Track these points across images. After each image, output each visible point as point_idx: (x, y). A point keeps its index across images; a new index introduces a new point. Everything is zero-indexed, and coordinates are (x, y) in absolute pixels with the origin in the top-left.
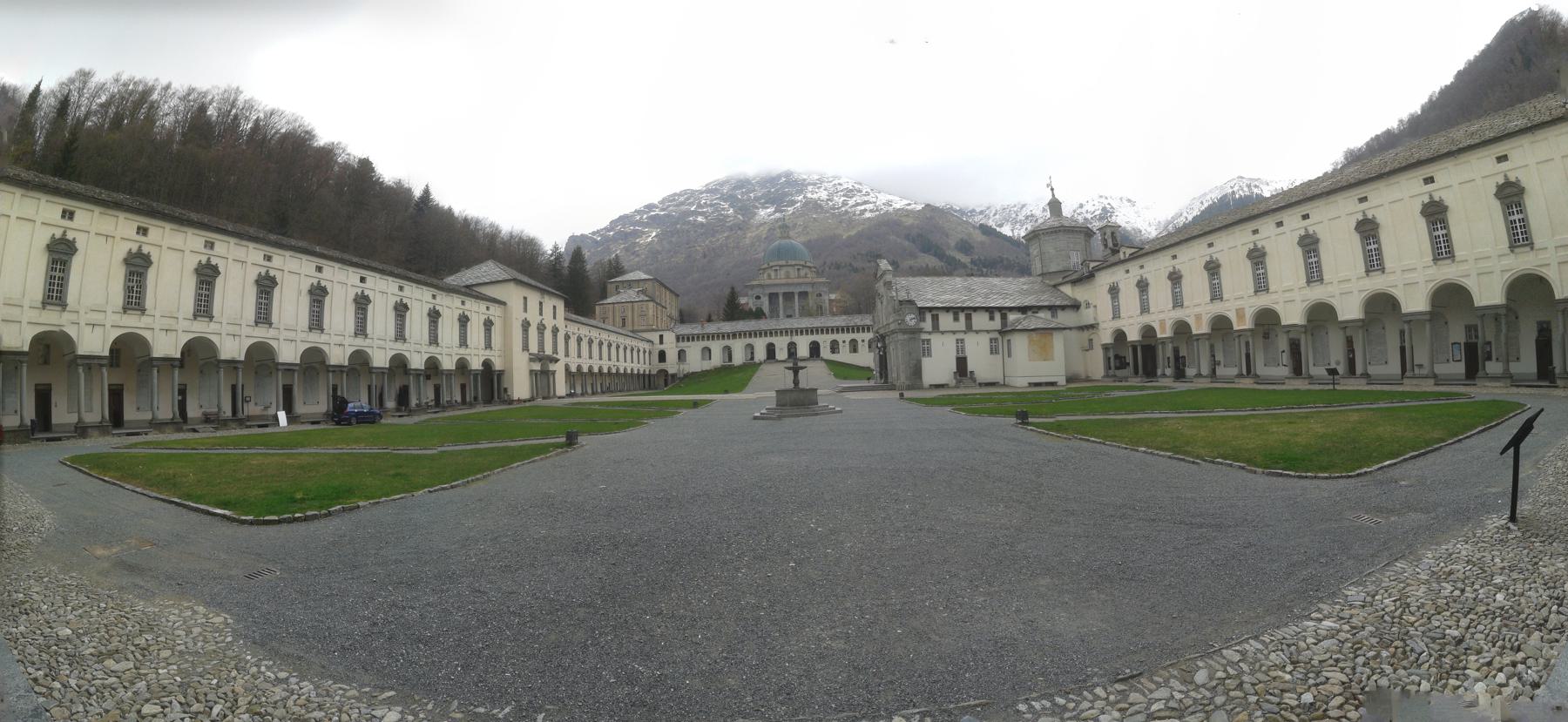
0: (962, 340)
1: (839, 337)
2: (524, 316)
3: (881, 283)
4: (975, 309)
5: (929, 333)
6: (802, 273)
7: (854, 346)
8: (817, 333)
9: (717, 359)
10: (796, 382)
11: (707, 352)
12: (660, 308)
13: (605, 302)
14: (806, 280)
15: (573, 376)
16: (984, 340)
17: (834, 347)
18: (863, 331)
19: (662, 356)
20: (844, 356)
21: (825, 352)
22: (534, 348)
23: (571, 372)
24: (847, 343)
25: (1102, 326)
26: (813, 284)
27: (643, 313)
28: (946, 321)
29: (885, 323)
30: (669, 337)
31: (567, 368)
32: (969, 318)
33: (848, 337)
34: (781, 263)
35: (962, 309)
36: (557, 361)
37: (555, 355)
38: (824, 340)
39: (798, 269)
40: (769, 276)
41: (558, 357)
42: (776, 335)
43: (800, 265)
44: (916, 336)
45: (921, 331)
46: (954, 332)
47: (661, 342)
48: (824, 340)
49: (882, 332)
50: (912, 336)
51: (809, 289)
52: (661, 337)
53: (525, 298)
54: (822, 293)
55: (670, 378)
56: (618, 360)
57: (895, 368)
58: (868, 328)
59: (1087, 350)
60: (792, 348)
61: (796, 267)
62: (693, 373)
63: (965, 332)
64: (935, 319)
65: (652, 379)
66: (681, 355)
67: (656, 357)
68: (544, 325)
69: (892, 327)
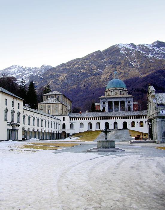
1: (135, 120)
2: (5, 107)
3: (150, 96)
6: (122, 93)
9: (86, 128)
11: (82, 124)
12: (64, 106)
13: (42, 103)
14: (125, 96)
15: (26, 132)
17: (133, 124)
19: (64, 126)
20: (137, 128)
21: (129, 127)
22: (9, 120)
23: (25, 131)
24: (139, 123)
26: (127, 98)
27: (57, 108)
29: (152, 114)
30: (67, 118)
31: (23, 129)
33: (139, 120)
36: (19, 126)
37: (18, 123)
38: (129, 121)
39: (121, 91)
40: (109, 94)
41: (19, 124)
43: (112, 90)
47: (64, 120)
48: (129, 121)
49: (150, 118)
50: (163, 119)
51: (125, 100)
52: (64, 118)
53: (6, 100)
54: (130, 102)
56: (45, 127)
57: (155, 134)
58: (144, 117)
60: (115, 123)
61: (120, 90)
62: (76, 133)
65: (60, 135)
66: (72, 126)
67: (61, 126)
68: (14, 111)
69: (155, 115)
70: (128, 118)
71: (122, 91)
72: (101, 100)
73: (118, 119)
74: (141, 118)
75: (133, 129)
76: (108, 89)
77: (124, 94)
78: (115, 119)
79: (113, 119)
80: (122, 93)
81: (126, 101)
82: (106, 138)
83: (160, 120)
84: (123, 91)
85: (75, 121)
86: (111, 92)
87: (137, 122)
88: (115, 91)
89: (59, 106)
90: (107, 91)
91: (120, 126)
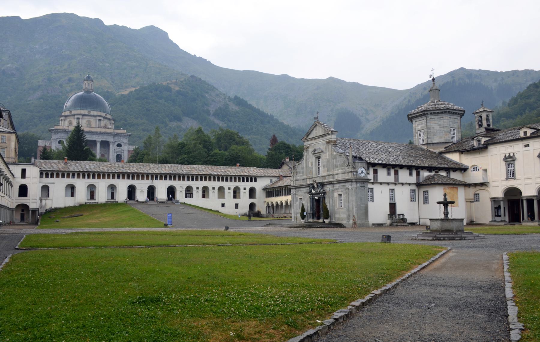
0: (393, 190)
1: (194, 184)
4: (402, 167)
5: (373, 183)
6: (103, 123)
7: (205, 192)
8: (175, 179)
10: (446, 214)
16: (407, 190)
18: (214, 180)
19: (23, 191)
20: (197, 200)
21: (180, 196)
25: (492, 184)
26: (116, 135)
28: (382, 174)
30: (33, 171)
32: (396, 173)
34: (83, 112)
35: (394, 166)
38: (180, 186)
39: (100, 120)
42: (138, 178)
44: (365, 185)
45: (367, 181)
46: (388, 184)
48: (180, 186)
50: (362, 185)
51: (110, 139)
52: (24, 171)
54: (122, 144)
55: (30, 212)
59: (471, 202)
61: (98, 118)
62: (56, 209)
63: (395, 184)
64: (375, 172)
70: (179, 179)
71: (102, 118)
72: (55, 133)
73: (156, 179)
74: (206, 180)
75: (188, 201)
76: (71, 112)
77: (105, 127)
78: (152, 179)
79: (148, 178)
80: (103, 123)
81: (114, 143)
82: (446, 214)
83: (359, 185)
84: (105, 120)
85: (54, 180)
86: (78, 119)
87: (198, 188)
88: (87, 118)
89: (9, 140)
90: (66, 116)
91: (161, 194)
